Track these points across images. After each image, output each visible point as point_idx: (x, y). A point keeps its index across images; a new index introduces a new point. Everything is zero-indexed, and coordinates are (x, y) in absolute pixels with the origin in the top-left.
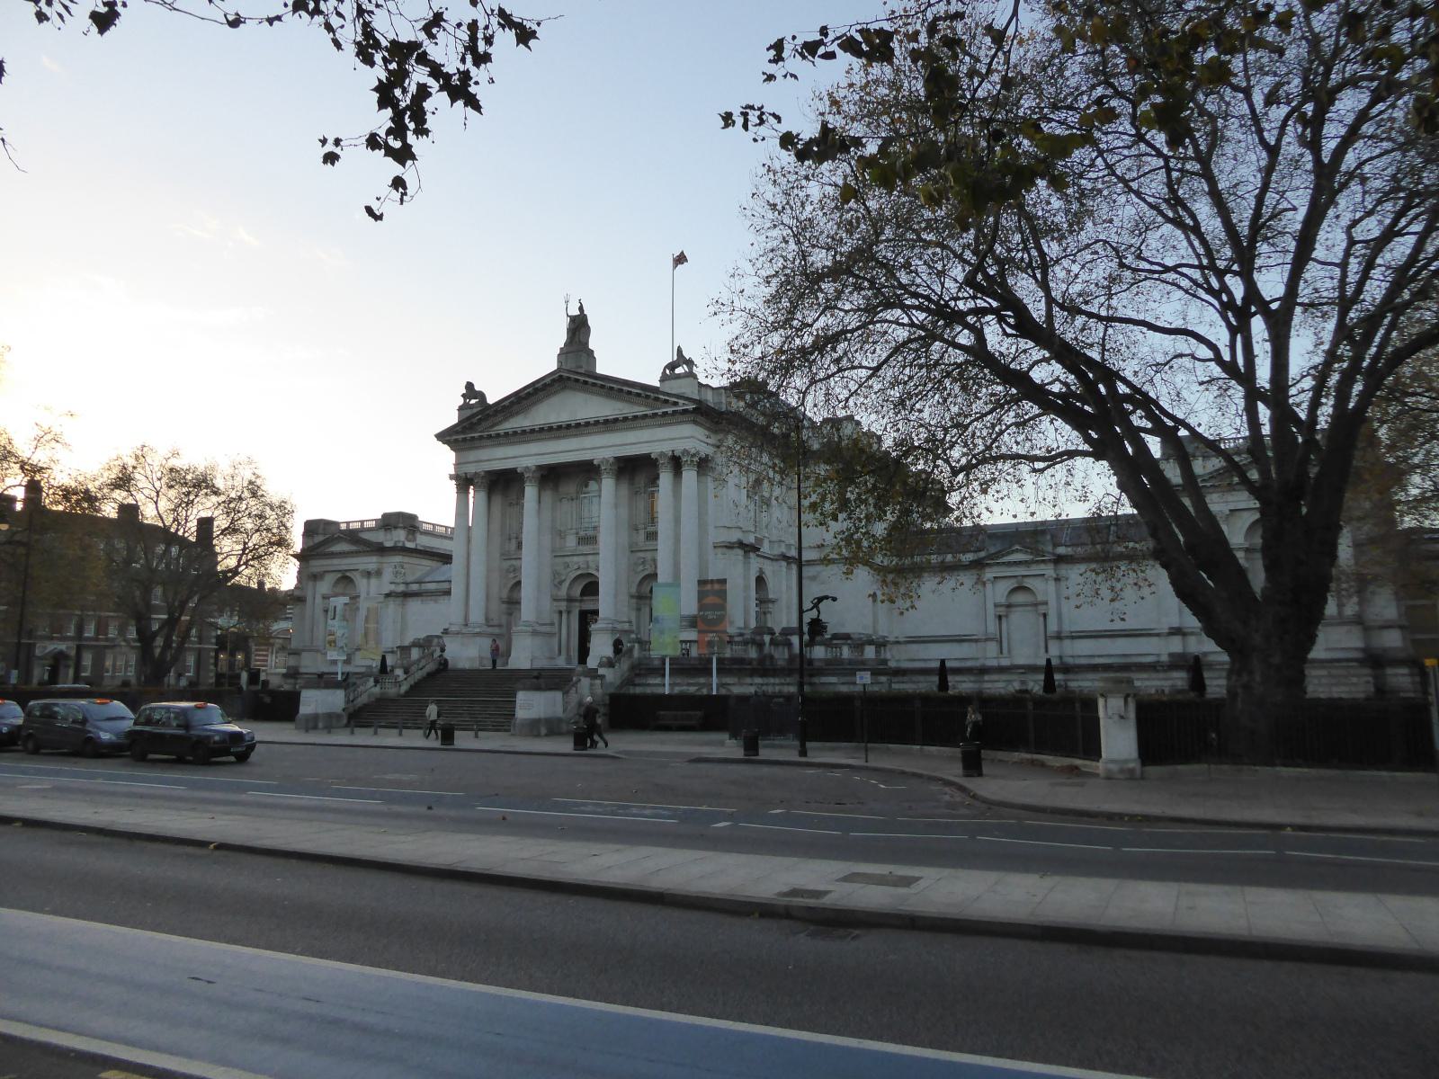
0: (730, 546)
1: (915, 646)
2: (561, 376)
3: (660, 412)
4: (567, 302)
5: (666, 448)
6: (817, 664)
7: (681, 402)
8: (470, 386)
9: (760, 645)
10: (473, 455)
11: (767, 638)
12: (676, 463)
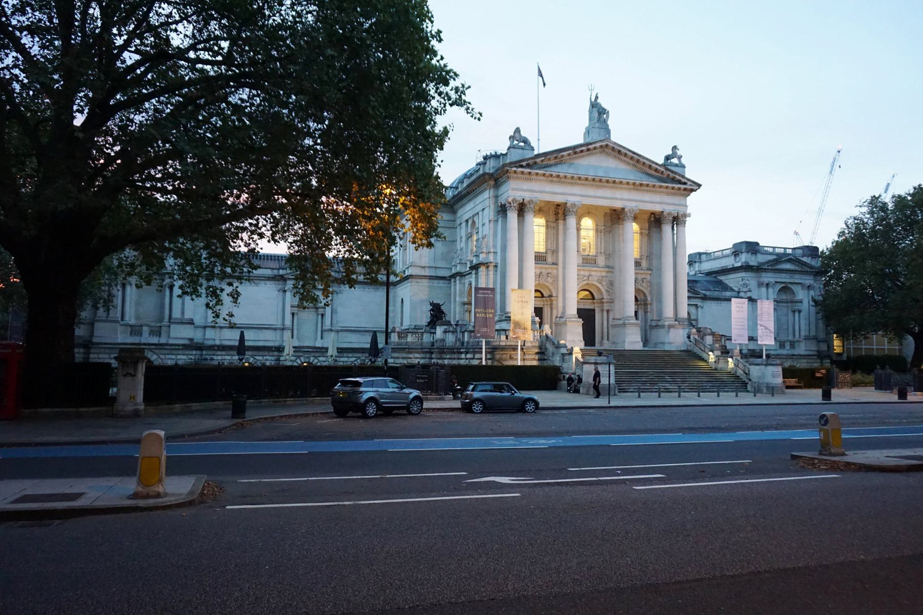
7: (689, 183)
8: (518, 130)
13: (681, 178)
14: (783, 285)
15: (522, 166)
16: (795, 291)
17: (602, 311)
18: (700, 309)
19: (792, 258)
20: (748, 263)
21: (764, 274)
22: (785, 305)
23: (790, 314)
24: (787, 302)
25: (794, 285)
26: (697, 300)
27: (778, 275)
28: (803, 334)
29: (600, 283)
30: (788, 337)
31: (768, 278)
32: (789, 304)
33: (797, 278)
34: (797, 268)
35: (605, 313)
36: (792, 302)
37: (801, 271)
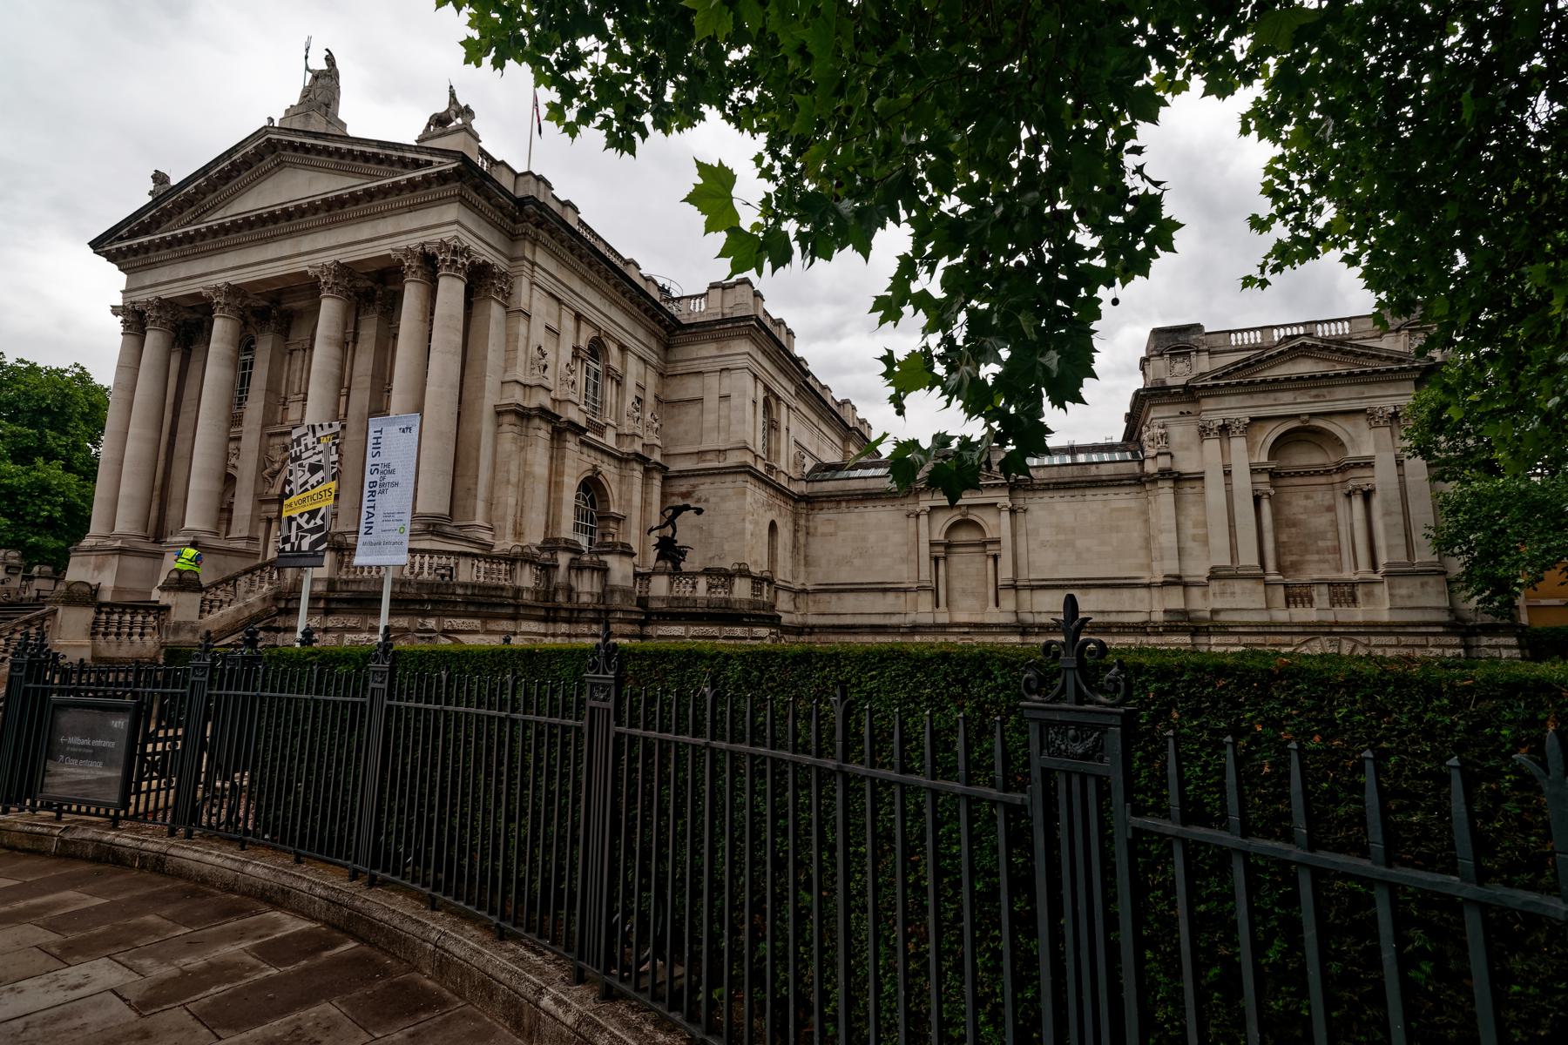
0: (523, 415)
1: (825, 597)
2: (269, 140)
3: (402, 178)
4: (307, 50)
5: (413, 241)
6: (655, 605)
9: (548, 569)
10: (149, 278)
11: (563, 559)
12: (429, 264)
13: (401, 154)
16: (1344, 438)
18: (1020, 516)
20: (1163, 382)
21: (1208, 404)
22: (1322, 480)
23: (1341, 502)
24: (1328, 472)
25: (1338, 420)
26: (994, 493)
27: (1260, 399)
28: (1383, 559)
30: (1339, 569)
31: (1217, 411)
32: (1337, 478)
33: (1343, 398)
34: (1341, 369)
36: (1343, 469)
37: (1350, 374)
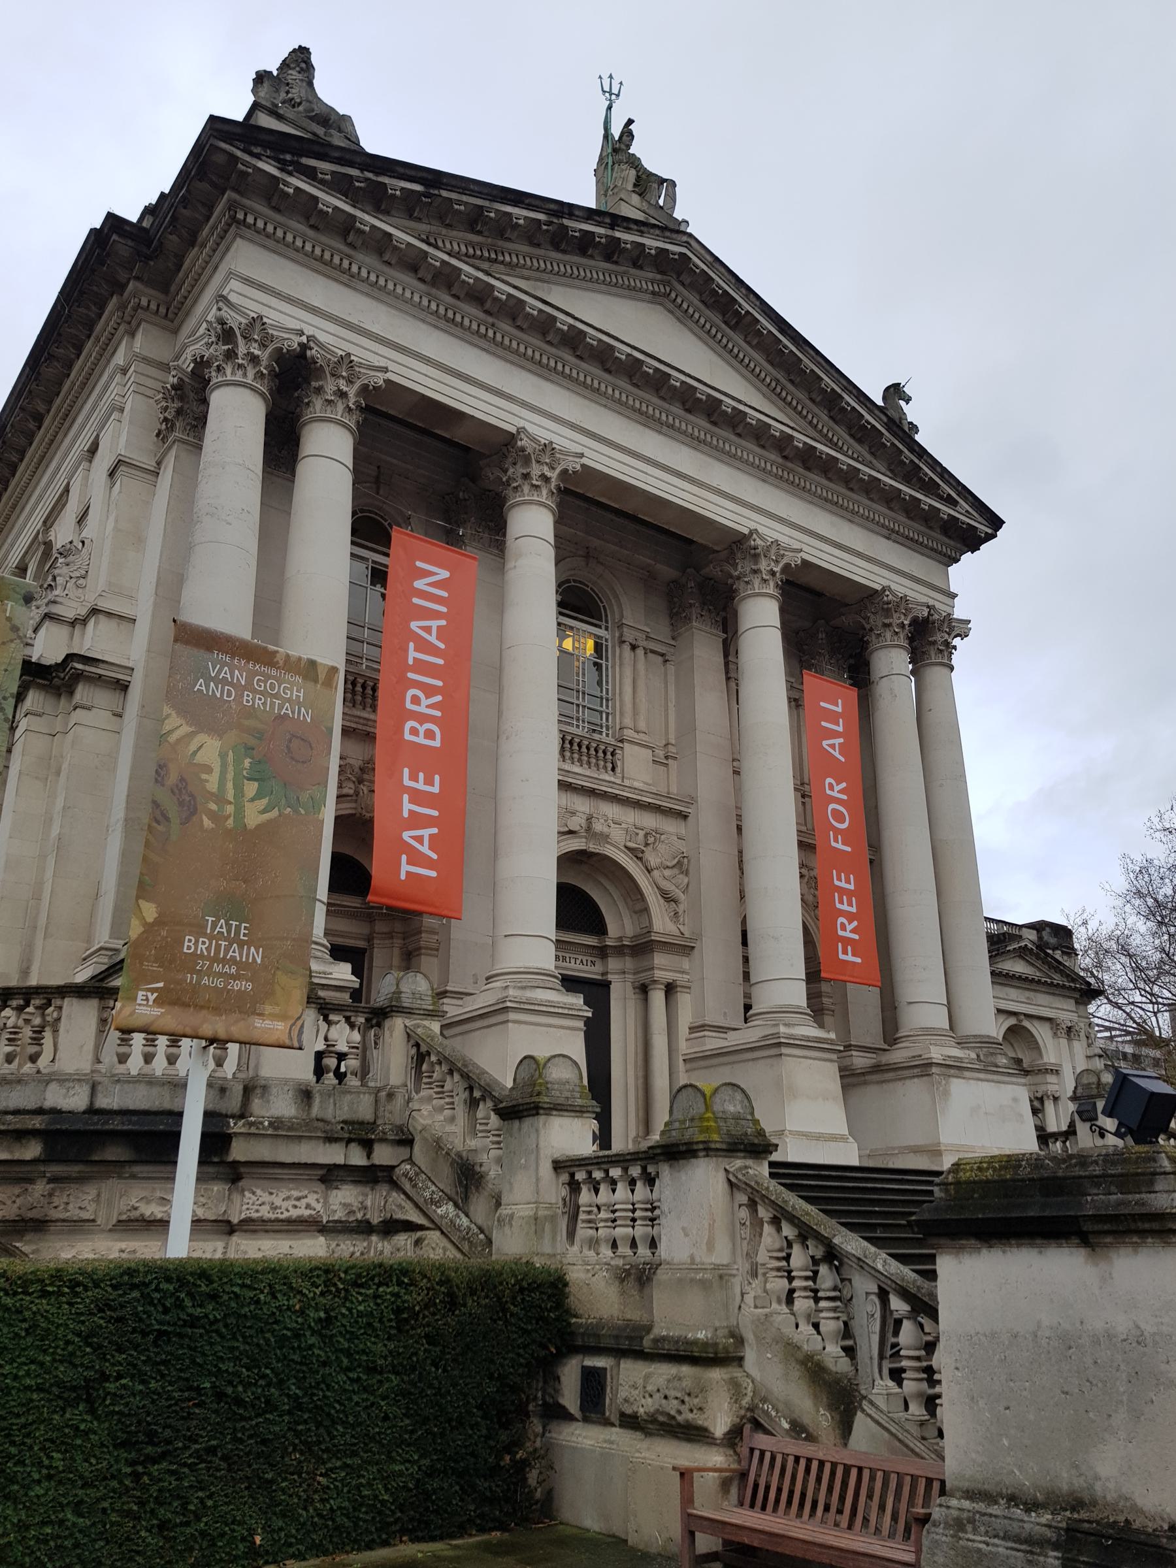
8: (300, 59)
14: (1012, 1021)
15: (310, 174)
17: (644, 990)
19: (1030, 946)
25: (1036, 1023)
29: (637, 854)
35: (658, 997)
